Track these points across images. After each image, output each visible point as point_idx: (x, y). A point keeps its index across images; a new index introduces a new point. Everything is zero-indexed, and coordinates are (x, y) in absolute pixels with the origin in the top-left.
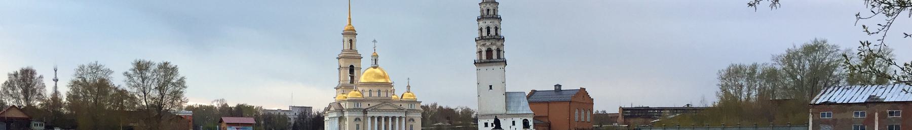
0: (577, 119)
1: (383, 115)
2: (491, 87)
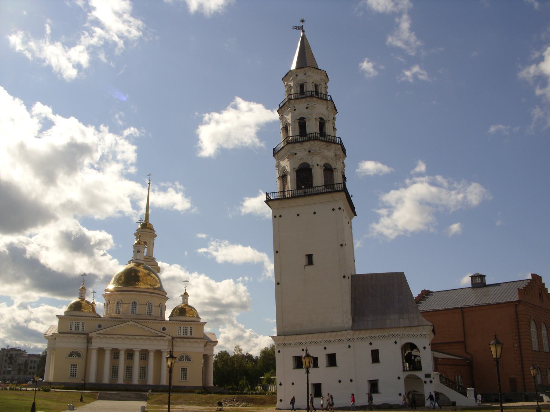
0: (535, 347)
1: (123, 345)
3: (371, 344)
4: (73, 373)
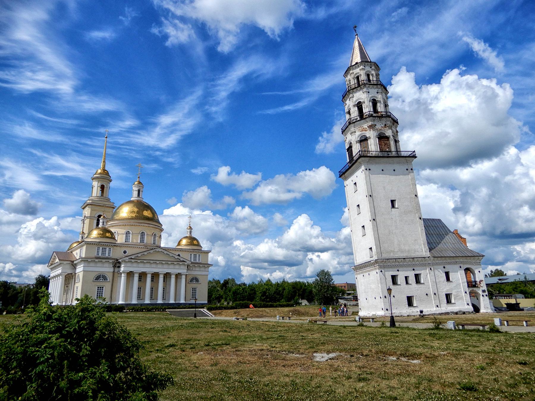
1: (150, 269)
2: (393, 202)
3: (444, 267)
4: (100, 294)
